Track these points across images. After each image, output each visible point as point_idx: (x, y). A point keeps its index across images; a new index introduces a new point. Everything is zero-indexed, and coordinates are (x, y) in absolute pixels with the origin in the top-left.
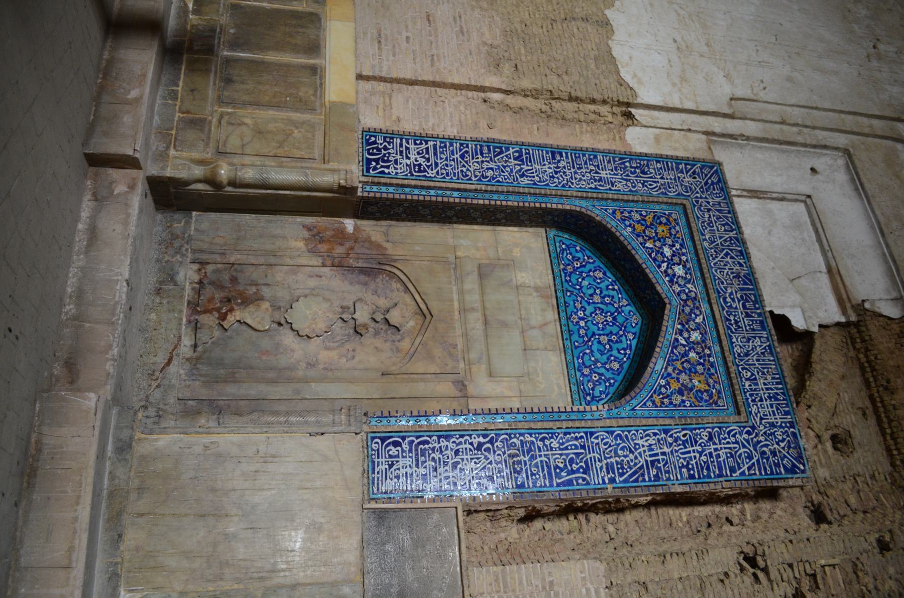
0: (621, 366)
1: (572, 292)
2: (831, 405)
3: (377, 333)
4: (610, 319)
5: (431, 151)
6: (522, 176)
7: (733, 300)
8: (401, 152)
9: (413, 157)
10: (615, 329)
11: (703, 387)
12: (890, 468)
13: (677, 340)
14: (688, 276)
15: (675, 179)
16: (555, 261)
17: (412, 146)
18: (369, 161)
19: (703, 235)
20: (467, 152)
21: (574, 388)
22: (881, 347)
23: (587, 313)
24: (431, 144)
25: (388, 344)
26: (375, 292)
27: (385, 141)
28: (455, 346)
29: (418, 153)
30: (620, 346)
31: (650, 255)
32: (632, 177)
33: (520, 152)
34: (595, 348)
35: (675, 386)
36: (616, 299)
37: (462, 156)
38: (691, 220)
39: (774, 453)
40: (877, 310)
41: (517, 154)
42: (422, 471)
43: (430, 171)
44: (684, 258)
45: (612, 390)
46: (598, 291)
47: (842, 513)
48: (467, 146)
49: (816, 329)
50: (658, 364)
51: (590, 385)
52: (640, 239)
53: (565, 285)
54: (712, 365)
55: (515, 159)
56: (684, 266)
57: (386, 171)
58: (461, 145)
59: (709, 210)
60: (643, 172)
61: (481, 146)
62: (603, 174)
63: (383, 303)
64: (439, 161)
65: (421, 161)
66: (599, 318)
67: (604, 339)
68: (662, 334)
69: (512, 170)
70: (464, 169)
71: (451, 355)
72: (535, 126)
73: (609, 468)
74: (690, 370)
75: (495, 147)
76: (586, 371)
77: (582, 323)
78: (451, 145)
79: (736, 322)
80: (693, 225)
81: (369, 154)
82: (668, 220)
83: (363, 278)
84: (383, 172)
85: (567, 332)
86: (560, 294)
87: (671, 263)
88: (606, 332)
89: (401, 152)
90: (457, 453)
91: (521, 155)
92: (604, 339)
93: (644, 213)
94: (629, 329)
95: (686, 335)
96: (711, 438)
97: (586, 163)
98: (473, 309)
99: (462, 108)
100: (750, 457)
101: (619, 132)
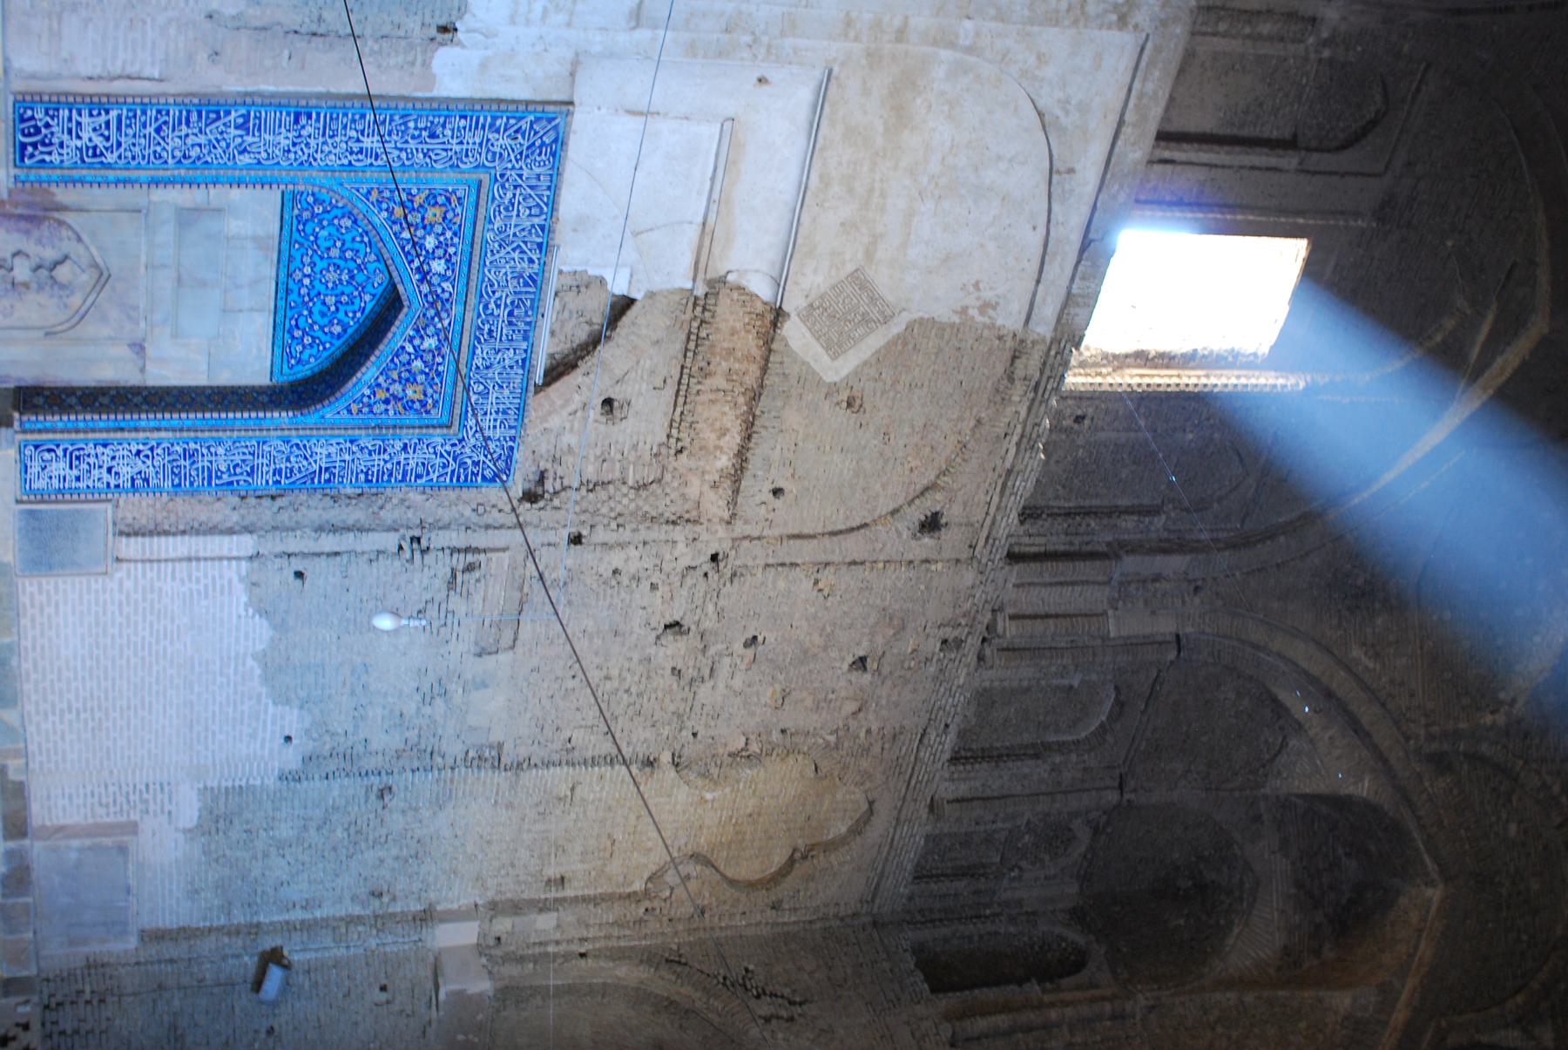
0: (345, 331)
1: (302, 245)
2: (618, 373)
3: (41, 288)
4: (345, 277)
5: (113, 126)
6: (241, 153)
7: (498, 306)
8: (70, 131)
9: (85, 135)
10: (349, 289)
11: (416, 397)
12: (664, 439)
13: (403, 348)
14: (449, 273)
15: (481, 144)
16: (288, 205)
17: (85, 120)
18: (23, 146)
19: (490, 222)
20: (166, 123)
21: (278, 351)
22: (723, 326)
23: (317, 269)
24: (114, 114)
25: (55, 300)
26: (39, 242)
27: (47, 113)
28: (136, 308)
29: (95, 130)
30: (349, 308)
31: (403, 248)
32: (413, 144)
33: (246, 117)
34: (316, 311)
35: (382, 395)
36: (362, 254)
37: (158, 130)
38: (482, 202)
39: (476, 464)
40: (744, 283)
41: (240, 121)
42: (75, 472)
43: (108, 155)
44: (451, 250)
45: (326, 354)
46: (339, 244)
47: (566, 483)
48: (168, 114)
49: (638, 295)
50: (369, 372)
51: (299, 348)
52: (397, 228)
53: (296, 235)
54: (439, 374)
55: (237, 128)
56: (448, 261)
57: (47, 158)
58: (159, 112)
59: (515, 187)
60: (433, 136)
61: (189, 112)
62: (367, 142)
63: (50, 254)
64: (123, 140)
65: (98, 141)
66: (332, 276)
67: (331, 300)
68: (386, 341)
69: (228, 146)
70: (159, 149)
71: (129, 317)
72: (286, 53)
73: (277, 472)
74: (407, 380)
75: (208, 112)
76: (298, 333)
77: (307, 281)
78: (144, 113)
79: (490, 331)
80: (482, 210)
81: (24, 135)
82: (448, 199)
83: (23, 225)
84: (43, 161)
85: (283, 290)
86: (285, 246)
87: (431, 256)
88: (337, 291)
89: (70, 131)
90: (113, 458)
91: (247, 120)
92: (331, 300)
93: (414, 191)
94: (369, 288)
95: (417, 342)
96: (405, 448)
97: (345, 127)
98: (164, 266)
99: (172, 31)
100: (445, 466)
101: (425, 52)
